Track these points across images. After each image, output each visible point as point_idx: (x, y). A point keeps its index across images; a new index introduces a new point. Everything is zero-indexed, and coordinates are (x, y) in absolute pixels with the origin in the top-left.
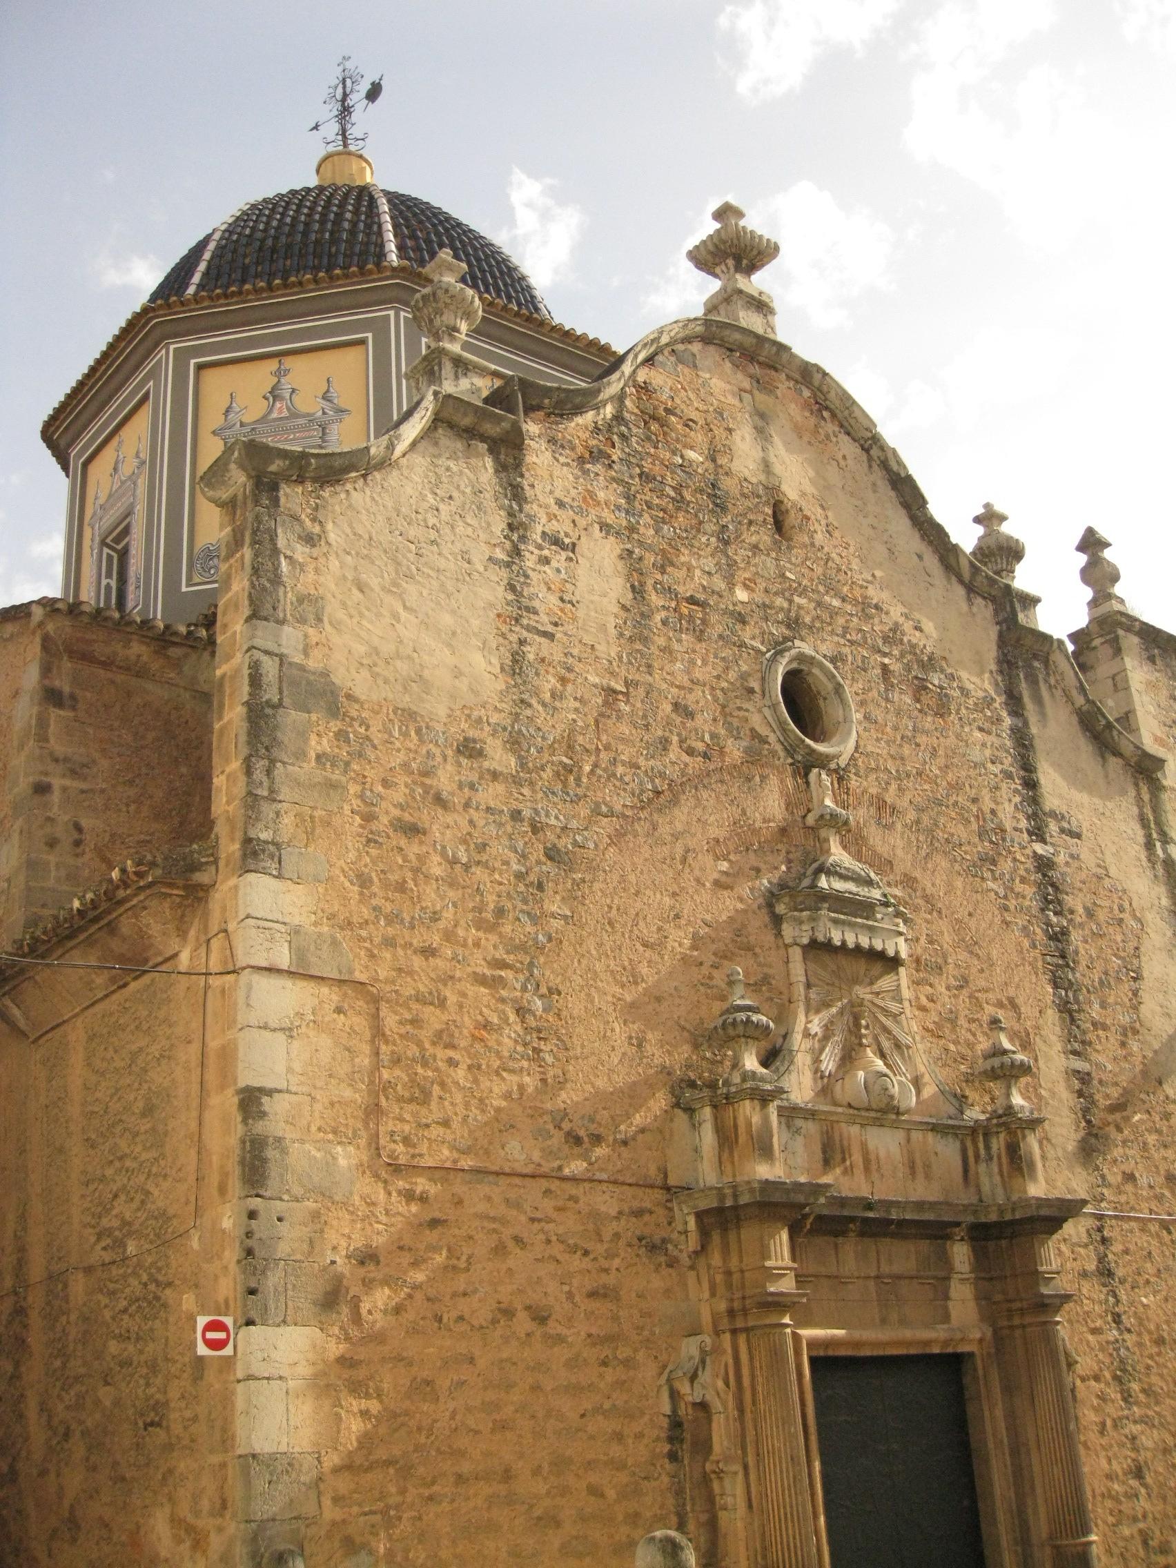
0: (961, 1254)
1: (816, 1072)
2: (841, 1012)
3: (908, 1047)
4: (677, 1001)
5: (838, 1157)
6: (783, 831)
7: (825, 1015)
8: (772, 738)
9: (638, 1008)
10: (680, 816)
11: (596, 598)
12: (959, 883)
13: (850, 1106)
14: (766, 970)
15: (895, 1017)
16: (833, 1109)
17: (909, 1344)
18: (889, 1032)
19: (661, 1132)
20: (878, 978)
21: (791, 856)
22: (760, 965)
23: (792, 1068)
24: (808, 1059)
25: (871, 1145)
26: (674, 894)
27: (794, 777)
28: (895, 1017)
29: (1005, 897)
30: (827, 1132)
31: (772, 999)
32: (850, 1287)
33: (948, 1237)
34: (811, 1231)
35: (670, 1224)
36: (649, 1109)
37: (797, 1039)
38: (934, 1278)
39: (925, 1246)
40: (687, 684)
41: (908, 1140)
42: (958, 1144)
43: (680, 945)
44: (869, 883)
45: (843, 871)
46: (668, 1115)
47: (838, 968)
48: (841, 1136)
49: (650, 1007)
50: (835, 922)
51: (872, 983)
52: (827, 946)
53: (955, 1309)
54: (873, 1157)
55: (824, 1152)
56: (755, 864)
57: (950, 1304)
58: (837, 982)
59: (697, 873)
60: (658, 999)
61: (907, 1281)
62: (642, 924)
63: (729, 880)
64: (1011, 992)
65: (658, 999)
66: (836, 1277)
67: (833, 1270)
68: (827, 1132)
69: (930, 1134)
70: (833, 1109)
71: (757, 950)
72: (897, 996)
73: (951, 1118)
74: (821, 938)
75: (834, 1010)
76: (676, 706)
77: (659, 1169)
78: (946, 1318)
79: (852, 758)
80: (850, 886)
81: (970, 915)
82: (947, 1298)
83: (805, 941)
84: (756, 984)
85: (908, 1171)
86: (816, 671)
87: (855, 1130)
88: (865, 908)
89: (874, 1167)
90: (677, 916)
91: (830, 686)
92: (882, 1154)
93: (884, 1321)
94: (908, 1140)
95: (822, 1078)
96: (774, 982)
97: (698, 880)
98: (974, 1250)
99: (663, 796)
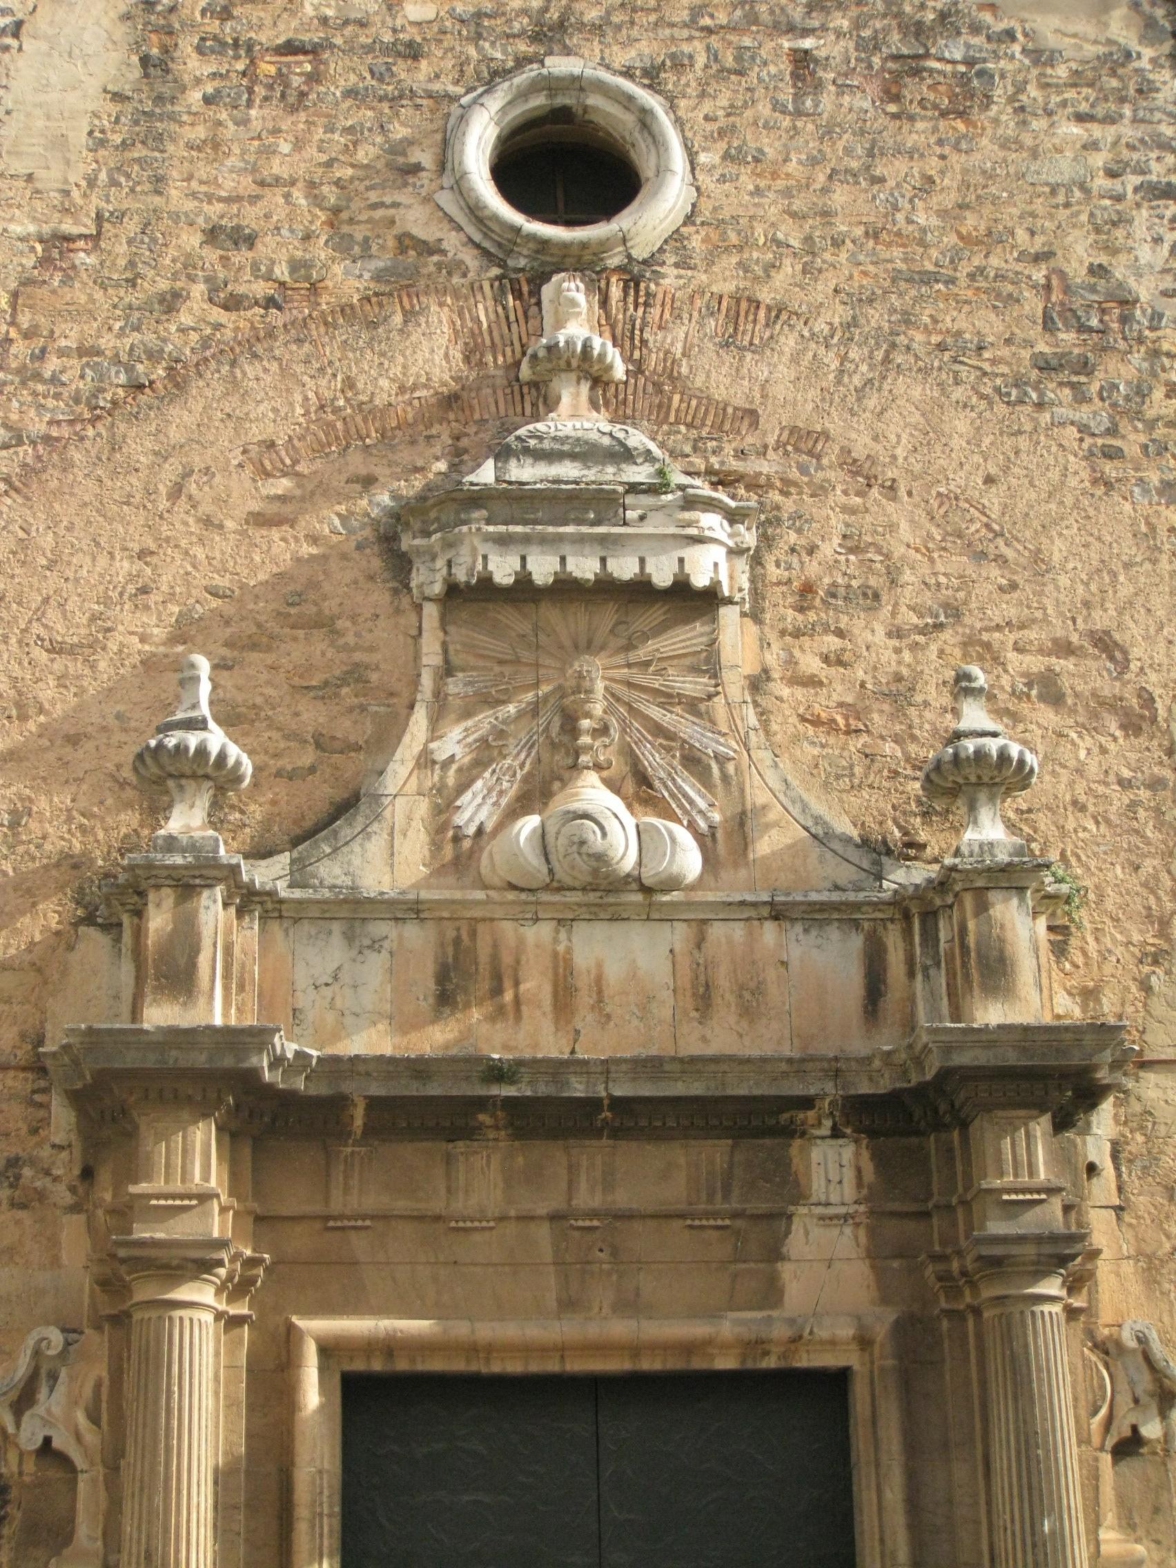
0: (832, 1167)
1: (441, 829)
2: (534, 710)
3: (721, 760)
4: (118, 737)
5: (485, 985)
6: (450, 401)
7: (484, 721)
8: (451, 241)
9: (21, 760)
10: (181, 419)
11: (54, 96)
12: (961, 424)
13: (512, 887)
14: (358, 656)
15: (693, 706)
16: (480, 895)
17: (635, 1350)
18: (670, 736)
19: (39, 970)
20: (645, 637)
21: (464, 442)
22: (346, 648)
23: (375, 827)
24: (423, 807)
25: (583, 958)
26: (143, 554)
27: (499, 299)
28: (693, 706)
29: (1112, 431)
30: (457, 941)
31: (363, 708)
32: (477, 1237)
33: (790, 1132)
34: (369, 1131)
35: (34, 1131)
36: (17, 932)
37: (399, 772)
38: (735, 1215)
39: (715, 1153)
40: (254, 190)
41: (700, 942)
42: (857, 942)
43: (143, 640)
44: (624, 455)
45: (547, 445)
46: (64, 940)
47: (536, 628)
48: (495, 946)
49: (51, 756)
50: (503, 541)
51: (629, 647)
52: (484, 590)
53: (798, 1284)
54: (583, 982)
55: (442, 976)
56: (363, 471)
57: (786, 1270)
58: (527, 656)
59: (205, 508)
60: (73, 740)
61: (651, 1224)
62: (52, 615)
63: (288, 509)
64: (1101, 620)
65: (73, 740)
66: (438, 1218)
67: (437, 1206)
68: (457, 941)
69: (769, 926)
70: (480, 895)
71: (340, 624)
72: (709, 663)
73: (837, 888)
74: (461, 575)
75: (512, 709)
76: (213, 235)
77: (23, 1036)
78: (771, 1294)
79: (676, 237)
80: (568, 470)
81: (989, 480)
82: (775, 1253)
83: (437, 588)
84: (326, 684)
85: (689, 1003)
86: (593, 100)
87: (539, 934)
88: (602, 504)
89: (585, 999)
90: (144, 590)
91: (629, 119)
92: (614, 973)
93: (569, 1305)
94: (700, 942)
95: (457, 839)
96: (374, 677)
97: (207, 522)
98: (879, 1158)
99: (154, 385)
